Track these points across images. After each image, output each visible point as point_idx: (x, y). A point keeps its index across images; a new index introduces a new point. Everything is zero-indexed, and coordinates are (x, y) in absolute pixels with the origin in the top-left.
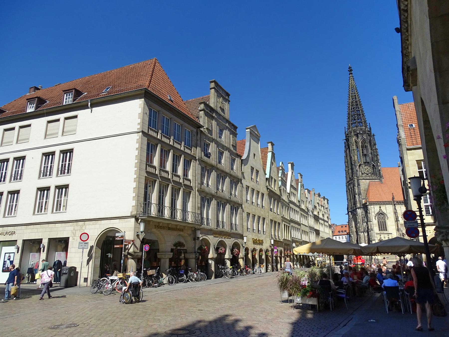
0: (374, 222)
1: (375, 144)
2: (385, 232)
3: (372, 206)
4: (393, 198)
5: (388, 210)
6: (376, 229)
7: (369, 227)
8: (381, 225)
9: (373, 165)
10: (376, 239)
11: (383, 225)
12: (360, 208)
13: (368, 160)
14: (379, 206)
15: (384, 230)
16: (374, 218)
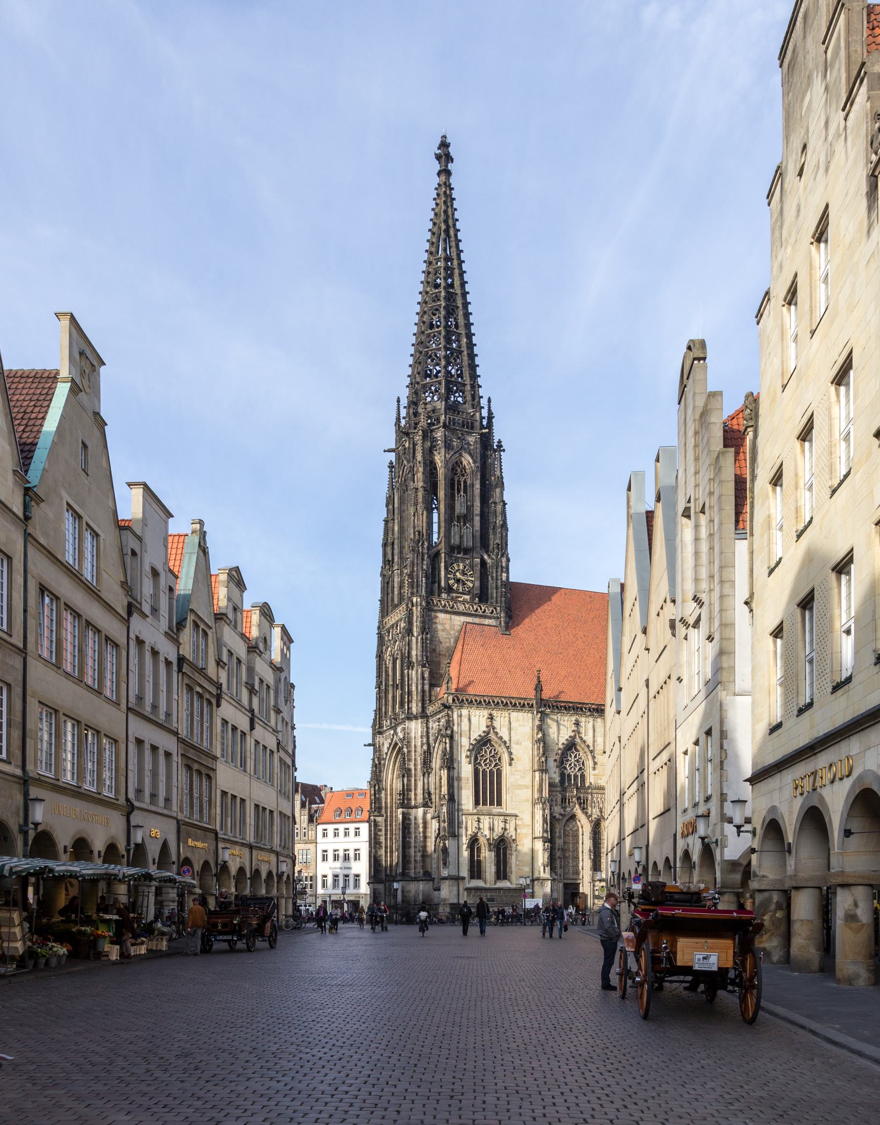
0: (466, 770)
2: (495, 810)
3: (465, 712)
4: (539, 688)
5: (518, 729)
12: (416, 718)
13: (468, 543)
14: (485, 713)
15: (492, 804)
16: (464, 755)
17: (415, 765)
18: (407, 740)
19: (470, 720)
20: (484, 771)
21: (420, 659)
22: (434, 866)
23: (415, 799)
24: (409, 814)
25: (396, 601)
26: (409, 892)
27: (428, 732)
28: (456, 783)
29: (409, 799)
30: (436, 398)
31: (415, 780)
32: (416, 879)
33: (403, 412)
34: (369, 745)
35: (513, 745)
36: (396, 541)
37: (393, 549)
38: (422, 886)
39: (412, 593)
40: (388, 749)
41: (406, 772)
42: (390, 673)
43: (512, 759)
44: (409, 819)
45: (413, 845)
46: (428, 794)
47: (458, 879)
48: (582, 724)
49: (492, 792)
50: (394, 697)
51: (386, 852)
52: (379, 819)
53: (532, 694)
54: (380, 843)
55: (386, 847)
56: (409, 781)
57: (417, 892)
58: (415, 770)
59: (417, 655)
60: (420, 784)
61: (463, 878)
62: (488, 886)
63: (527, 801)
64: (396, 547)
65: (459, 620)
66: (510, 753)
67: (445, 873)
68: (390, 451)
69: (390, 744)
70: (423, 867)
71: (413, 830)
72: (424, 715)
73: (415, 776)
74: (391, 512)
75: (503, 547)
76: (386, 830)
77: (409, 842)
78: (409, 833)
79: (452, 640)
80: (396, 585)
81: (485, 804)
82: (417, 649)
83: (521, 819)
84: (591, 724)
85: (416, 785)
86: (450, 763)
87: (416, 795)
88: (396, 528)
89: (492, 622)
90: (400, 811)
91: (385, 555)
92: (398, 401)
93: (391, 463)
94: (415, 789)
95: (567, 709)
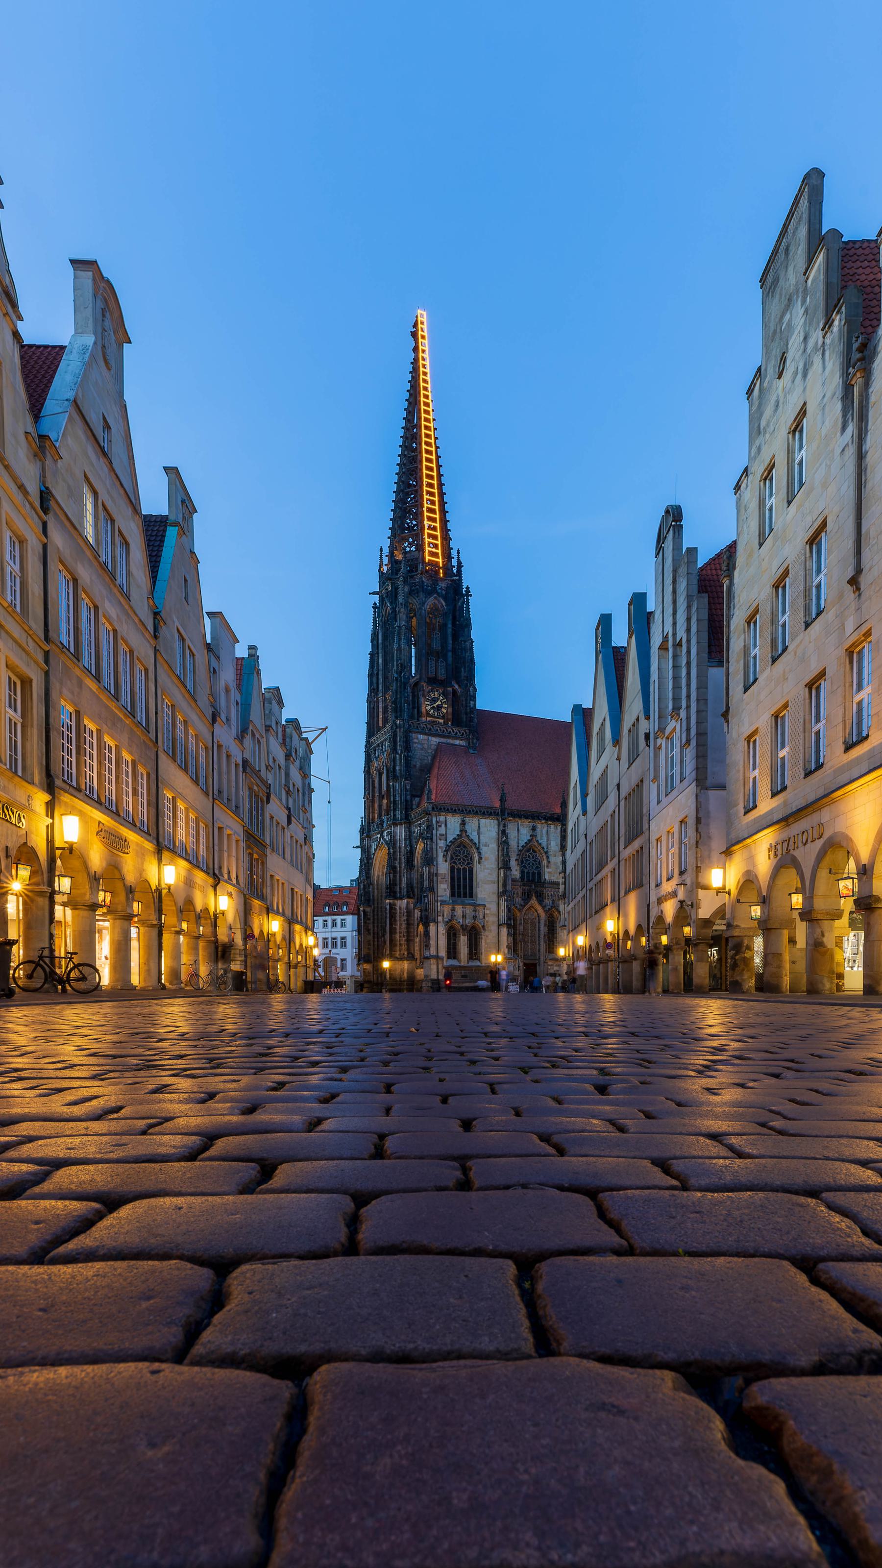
0: (443, 867)
1: (468, 625)
3: (442, 818)
5: (485, 831)
6: (444, 889)
7: (426, 884)
8: (459, 879)
9: (454, 692)
10: (440, 919)
11: (465, 879)
13: (442, 675)
15: (465, 896)
16: (441, 855)
17: (400, 863)
18: (392, 844)
19: (446, 825)
20: (459, 870)
21: (403, 773)
22: (417, 948)
23: (400, 892)
24: (395, 905)
25: (381, 725)
27: (410, 836)
28: (435, 878)
29: (395, 892)
30: (413, 549)
31: (400, 876)
32: (401, 959)
33: (386, 560)
34: (357, 847)
35: (481, 847)
36: (380, 673)
37: (378, 679)
38: (406, 965)
39: (396, 717)
40: (375, 850)
41: (392, 868)
42: (377, 785)
43: (480, 858)
44: (395, 909)
45: (398, 931)
46: (410, 886)
47: (437, 958)
48: (538, 830)
49: (465, 886)
50: (380, 806)
51: (374, 938)
52: (368, 909)
53: (497, 804)
54: (369, 930)
56: (395, 876)
57: (402, 971)
58: (400, 867)
59: (400, 770)
60: (404, 880)
62: (462, 964)
63: (494, 893)
64: (380, 677)
65: (435, 740)
66: (480, 853)
67: (427, 954)
69: (377, 846)
70: (408, 949)
71: (398, 918)
72: (408, 821)
74: (375, 646)
75: (471, 677)
77: (395, 929)
78: (395, 921)
79: (430, 758)
80: (381, 710)
81: (459, 896)
82: (400, 765)
83: (489, 909)
84: (545, 829)
85: (400, 880)
86: (429, 860)
87: (400, 888)
88: (380, 661)
89: (462, 743)
91: (371, 683)
92: (381, 550)
93: (375, 604)
94: (400, 884)
95: (527, 817)
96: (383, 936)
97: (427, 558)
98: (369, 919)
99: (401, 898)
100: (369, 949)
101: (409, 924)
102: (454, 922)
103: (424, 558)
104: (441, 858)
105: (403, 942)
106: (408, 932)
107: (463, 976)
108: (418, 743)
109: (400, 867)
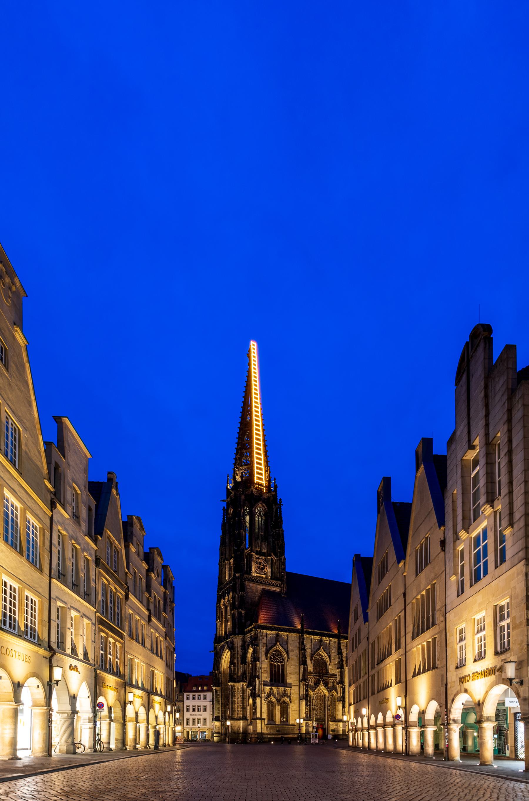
0: (265, 664)
10: (263, 695)
17: (237, 661)
26: (235, 727)
31: (238, 669)
32: (239, 719)
38: (241, 724)
44: (235, 689)
51: (222, 706)
52: (218, 688)
54: (218, 702)
55: (222, 704)
57: (239, 727)
58: (238, 663)
61: (264, 719)
68: (223, 500)
71: (236, 694)
73: (238, 666)
76: (222, 695)
77: (235, 701)
78: (235, 696)
79: (257, 598)
90: (230, 684)
96: (228, 705)
97: (256, 480)
98: (219, 695)
99: (239, 682)
100: (218, 713)
101: (243, 699)
102: (272, 697)
103: (254, 481)
104: (263, 658)
105: (239, 709)
106: (243, 703)
107: (277, 731)
108: (250, 589)
109: (238, 663)
